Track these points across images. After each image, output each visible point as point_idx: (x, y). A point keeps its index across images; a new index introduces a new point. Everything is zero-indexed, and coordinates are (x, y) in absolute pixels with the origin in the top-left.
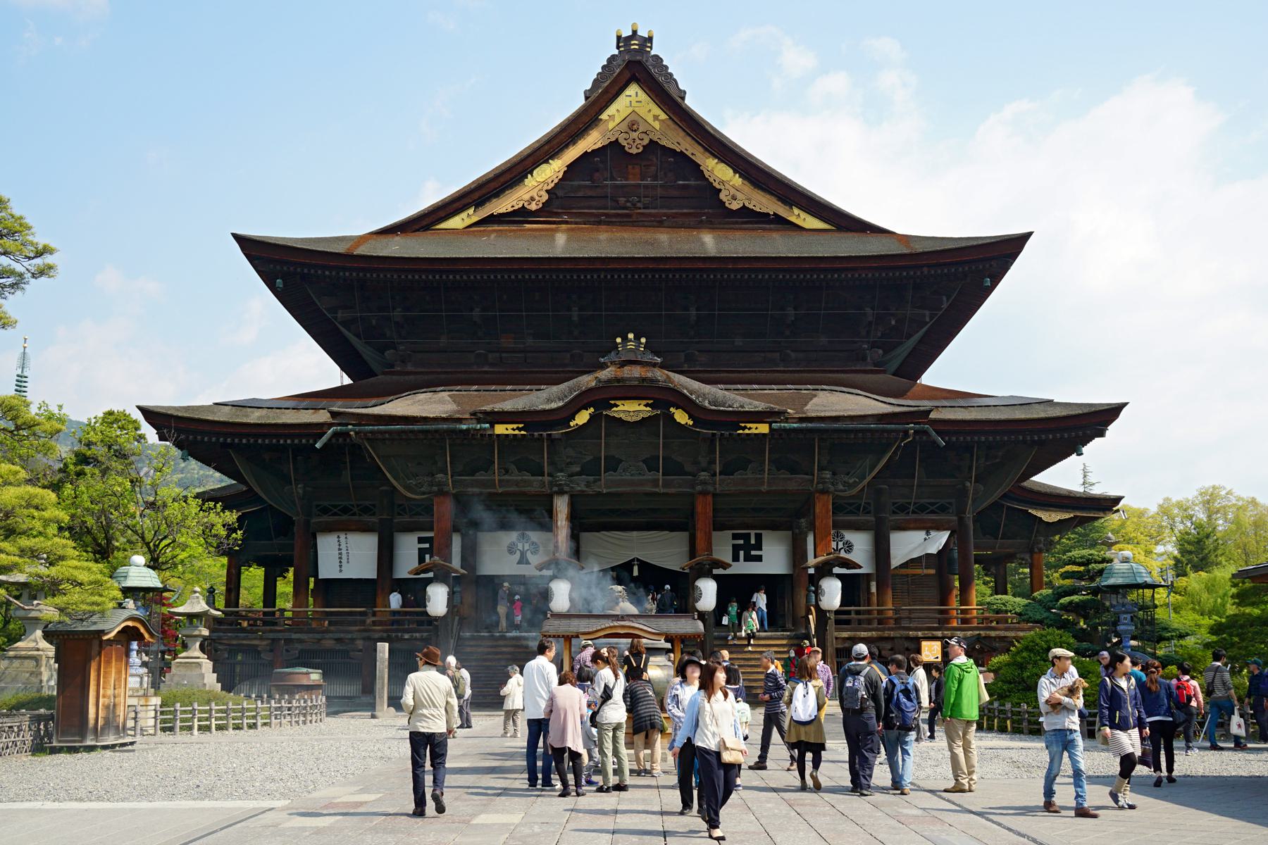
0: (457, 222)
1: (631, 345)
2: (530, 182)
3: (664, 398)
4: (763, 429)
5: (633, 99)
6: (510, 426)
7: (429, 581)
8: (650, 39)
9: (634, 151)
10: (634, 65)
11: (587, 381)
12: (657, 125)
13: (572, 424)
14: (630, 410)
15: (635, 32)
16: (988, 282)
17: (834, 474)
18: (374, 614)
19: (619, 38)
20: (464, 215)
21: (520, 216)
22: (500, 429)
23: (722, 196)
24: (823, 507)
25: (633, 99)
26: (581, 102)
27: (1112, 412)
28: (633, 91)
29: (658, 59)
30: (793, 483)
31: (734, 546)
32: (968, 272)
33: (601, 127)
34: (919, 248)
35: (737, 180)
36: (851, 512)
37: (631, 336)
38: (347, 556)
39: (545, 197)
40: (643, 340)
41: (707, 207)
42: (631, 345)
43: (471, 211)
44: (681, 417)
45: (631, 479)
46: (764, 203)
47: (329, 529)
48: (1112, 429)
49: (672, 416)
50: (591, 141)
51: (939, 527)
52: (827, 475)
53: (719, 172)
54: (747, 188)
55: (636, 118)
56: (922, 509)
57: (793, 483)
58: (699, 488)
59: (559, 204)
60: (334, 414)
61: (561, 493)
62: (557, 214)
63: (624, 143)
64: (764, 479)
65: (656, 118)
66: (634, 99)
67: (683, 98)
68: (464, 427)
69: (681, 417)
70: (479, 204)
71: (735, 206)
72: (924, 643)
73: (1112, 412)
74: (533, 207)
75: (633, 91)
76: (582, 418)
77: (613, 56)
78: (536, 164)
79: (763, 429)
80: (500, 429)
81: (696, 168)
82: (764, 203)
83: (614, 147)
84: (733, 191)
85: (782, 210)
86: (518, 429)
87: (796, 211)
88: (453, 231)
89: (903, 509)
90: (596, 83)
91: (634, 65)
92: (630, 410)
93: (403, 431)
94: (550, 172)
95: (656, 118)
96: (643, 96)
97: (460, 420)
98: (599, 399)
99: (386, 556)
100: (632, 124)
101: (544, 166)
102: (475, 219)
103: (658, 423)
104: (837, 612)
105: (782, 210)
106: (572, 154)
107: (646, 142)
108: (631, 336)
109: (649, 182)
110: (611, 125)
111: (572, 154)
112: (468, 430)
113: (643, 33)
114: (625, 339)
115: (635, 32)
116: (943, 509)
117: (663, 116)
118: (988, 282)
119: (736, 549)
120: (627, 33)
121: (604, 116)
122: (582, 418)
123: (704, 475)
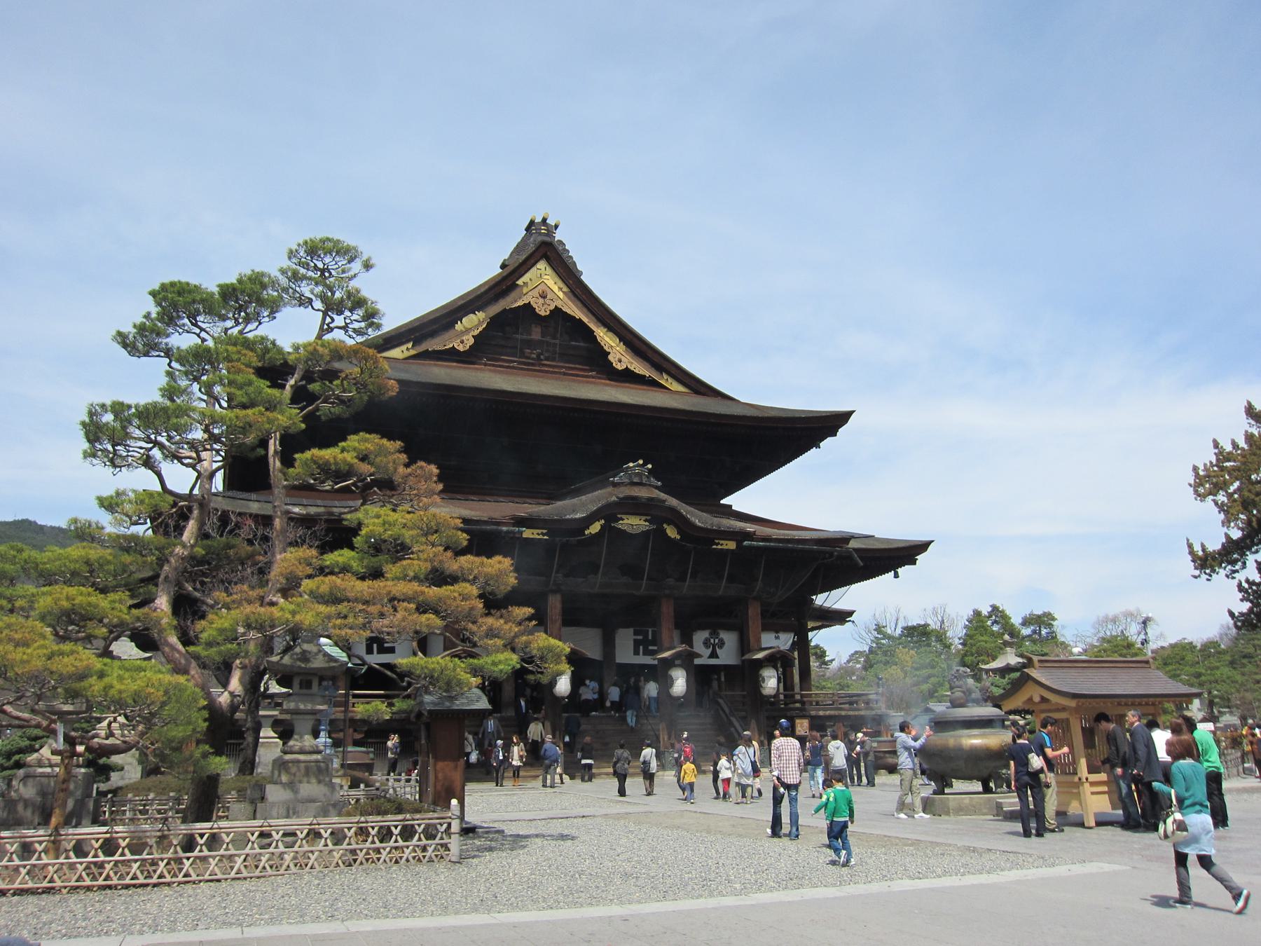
0: (396, 353)
2: (459, 326)
4: (731, 545)
6: (536, 531)
8: (556, 227)
9: (543, 313)
10: (542, 247)
13: (587, 532)
14: (633, 523)
15: (544, 220)
19: (532, 223)
20: (404, 347)
21: (451, 355)
22: (528, 533)
23: (610, 357)
24: (754, 611)
27: (923, 547)
28: (542, 265)
29: (560, 242)
31: (635, 641)
32: (789, 436)
39: (472, 341)
40: (650, 466)
41: (598, 362)
43: (410, 345)
44: (672, 532)
46: (639, 368)
51: (786, 629)
53: (606, 338)
55: (545, 288)
58: (667, 592)
61: (554, 592)
63: (535, 306)
68: (505, 529)
69: (672, 532)
71: (620, 367)
72: (798, 721)
73: (923, 547)
75: (542, 265)
76: (595, 528)
79: (731, 545)
80: (528, 533)
82: (639, 368)
83: (528, 306)
84: (618, 356)
86: (543, 534)
87: (665, 376)
91: (542, 247)
92: (633, 523)
94: (474, 323)
97: (498, 524)
98: (609, 513)
101: (471, 316)
102: (413, 352)
106: (495, 309)
107: (552, 307)
111: (495, 309)
112: (508, 532)
113: (551, 222)
115: (544, 220)
117: (565, 289)
119: (637, 644)
121: (520, 282)
122: (595, 528)
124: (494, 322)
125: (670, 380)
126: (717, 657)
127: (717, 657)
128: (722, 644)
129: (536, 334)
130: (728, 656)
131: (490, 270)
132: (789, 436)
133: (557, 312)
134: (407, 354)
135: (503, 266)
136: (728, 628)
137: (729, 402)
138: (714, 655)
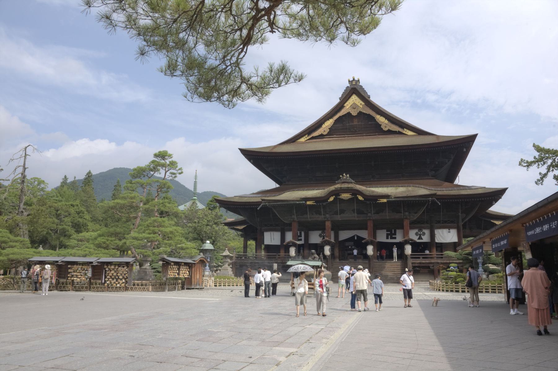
0: (303, 140)
1: (345, 178)
2: (324, 126)
3: (355, 193)
4: (385, 200)
5: (354, 99)
7: (291, 246)
8: (359, 81)
9: (355, 115)
11: (332, 188)
12: (361, 106)
15: (354, 79)
16: (465, 150)
17: (410, 213)
18: (279, 255)
19: (349, 81)
20: (304, 137)
22: (308, 203)
23: (382, 127)
24: (406, 223)
25: (354, 99)
26: (338, 101)
29: (361, 86)
30: (397, 216)
33: (345, 108)
34: (441, 140)
35: (386, 121)
36: (422, 224)
37: (344, 175)
38: (272, 238)
41: (377, 130)
42: (345, 178)
44: (360, 198)
45: (350, 216)
47: (268, 230)
48: (504, 197)
49: (357, 198)
50: (343, 112)
52: (407, 213)
53: (381, 119)
54: (390, 124)
56: (445, 222)
57: (397, 216)
59: (332, 132)
60: (263, 200)
61: (328, 220)
62: (333, 135)
64: (387, 215)
65: (361, 104)
66: (354, 99)
67: (369, 98)
69: (360, 198)
70: (309, 134)
71: (386, 129)
74: (325, 133)
76: (332, 199)
77: (348, 87)
78: (325, 121)
79: (385, 200)
80: (308, 203)
81: (373, 119)
83: (349, 114)
84: (385, 125)
85: (401, 130)
87: (405, 130)
88: (302, 143)
89: (439, 222)
90: (342, 95)
92: (346, 196)
93: (280, 204)
94: (329, 123)
95: (361, 104)
96: (356, 97)
98: (336, 193)
99: (283, 238)
100: (354, 106)
101: (328, 121)
102: (308, 138)
103: (354, 200)
104: (411, 255)
105: (401, 130)
106: (336, 117)
108: (344, 175)
109: (360, 123)
110: (347, 107)
111: (336, 117)
113: (356, 79)
114: (343, 176)
115: (354, 79)
116: (452, 222)
117: (363, 103)
118: (465, 150)
120: (351, 79)
121: (345, 105)
122: (332, 199)
123: (369, 214)
124: (336, 121)
125: (407, 131)
126: (422, 239)
127: (422, 239)
128: (424, 234)
129: (356, 122)
130: (426, 239)
131: (336, 101)
132: (459, 148)
133: (360, 113)
134: (306, 139)
135: (340, 99)
136: (425, 228)
137: (430, 137)
138: (420, 238)
